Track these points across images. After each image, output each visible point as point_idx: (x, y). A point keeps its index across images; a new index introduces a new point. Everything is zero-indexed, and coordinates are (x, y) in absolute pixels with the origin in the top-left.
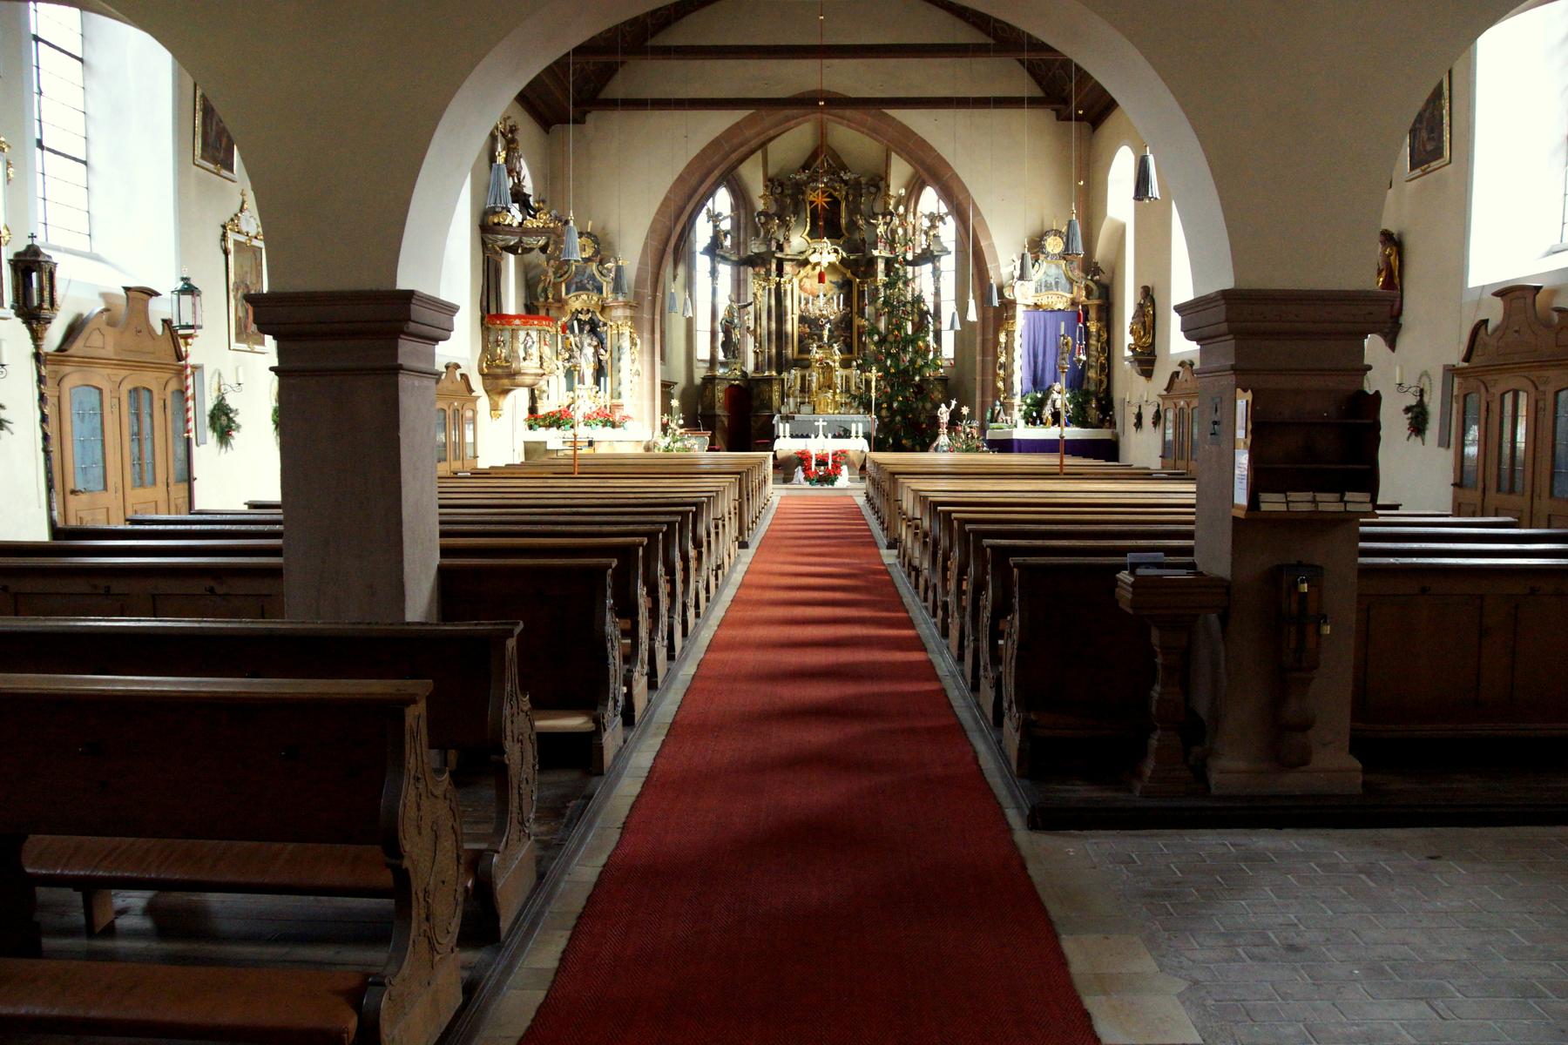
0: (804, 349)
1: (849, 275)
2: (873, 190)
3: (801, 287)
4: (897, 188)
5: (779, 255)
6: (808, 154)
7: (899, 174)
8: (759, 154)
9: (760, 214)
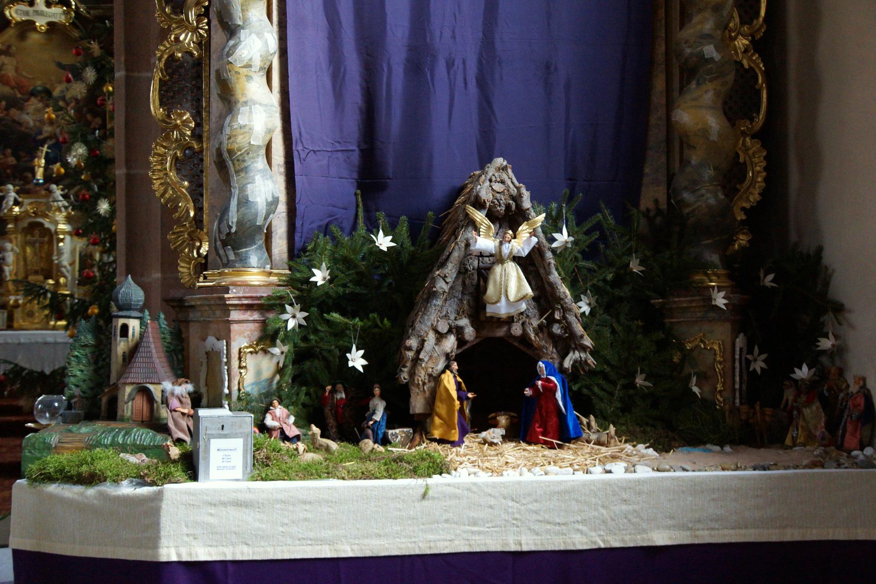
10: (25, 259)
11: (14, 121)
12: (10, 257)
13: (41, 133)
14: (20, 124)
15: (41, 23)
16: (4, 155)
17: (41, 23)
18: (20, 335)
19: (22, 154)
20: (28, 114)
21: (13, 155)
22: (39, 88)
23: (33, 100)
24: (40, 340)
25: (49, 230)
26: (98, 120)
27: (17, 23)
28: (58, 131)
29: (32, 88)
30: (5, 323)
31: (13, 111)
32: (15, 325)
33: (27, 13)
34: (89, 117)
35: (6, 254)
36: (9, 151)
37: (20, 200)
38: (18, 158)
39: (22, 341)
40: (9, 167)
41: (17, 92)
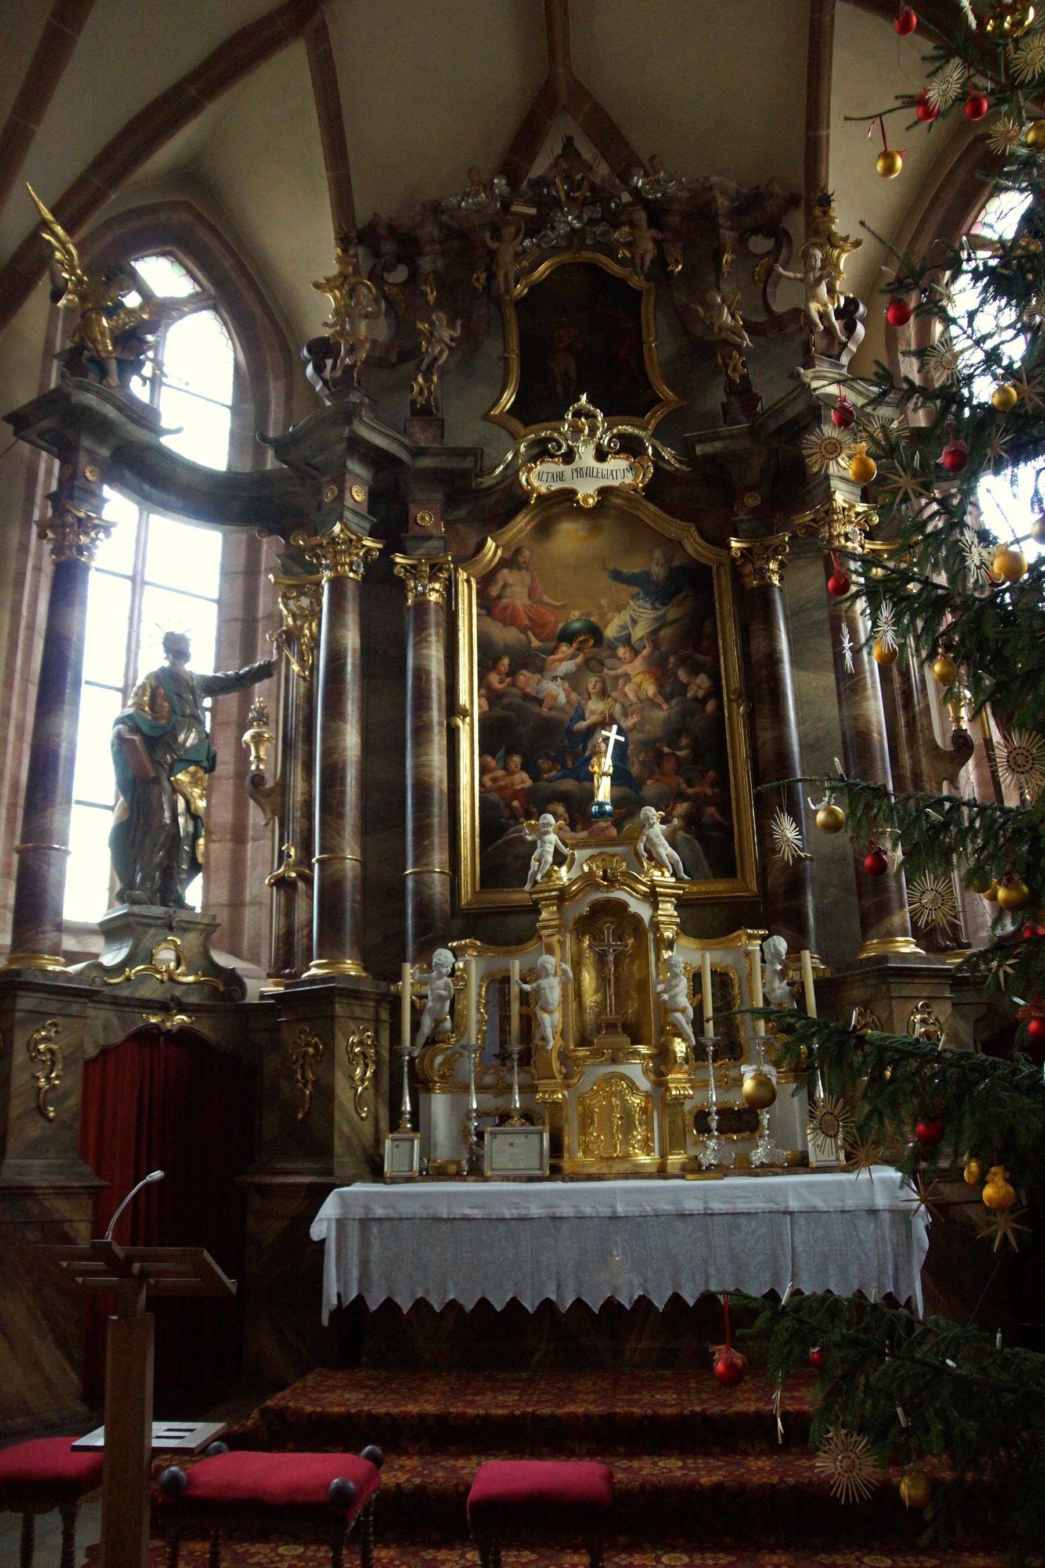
0: (504, 854)
1: (694, 545)
2: (759, 244)
3: (487, 604)
9: (322, 350)
10: (579, 994)
11: (526, 697)
12: (553, 990)
13: (583, 718)
14: (540, 702)
15: (587, 491)
16: (505, 768)
17: (587, 491)
18: (613, 1191)
19: (543, 763)
20: (554, 678)
21: (524, 767)
22: (577, 625)
23: (565, 649)
24: (667, 1207)
25: (637, 918)
26: (703, 681)
27: (539, 496)
28: (618, 708)
29: (561, 626)
30: (547, 1162)
31: (525, 677)
32: (567, 1165)
33: (561, 477)
34: (682, 675)
35: (544, 983)
36: (517, 759)
37: (566, 851)
38: (536, 775)
39: (620, 1210)
40: (516, 794)
41: (532, 638)
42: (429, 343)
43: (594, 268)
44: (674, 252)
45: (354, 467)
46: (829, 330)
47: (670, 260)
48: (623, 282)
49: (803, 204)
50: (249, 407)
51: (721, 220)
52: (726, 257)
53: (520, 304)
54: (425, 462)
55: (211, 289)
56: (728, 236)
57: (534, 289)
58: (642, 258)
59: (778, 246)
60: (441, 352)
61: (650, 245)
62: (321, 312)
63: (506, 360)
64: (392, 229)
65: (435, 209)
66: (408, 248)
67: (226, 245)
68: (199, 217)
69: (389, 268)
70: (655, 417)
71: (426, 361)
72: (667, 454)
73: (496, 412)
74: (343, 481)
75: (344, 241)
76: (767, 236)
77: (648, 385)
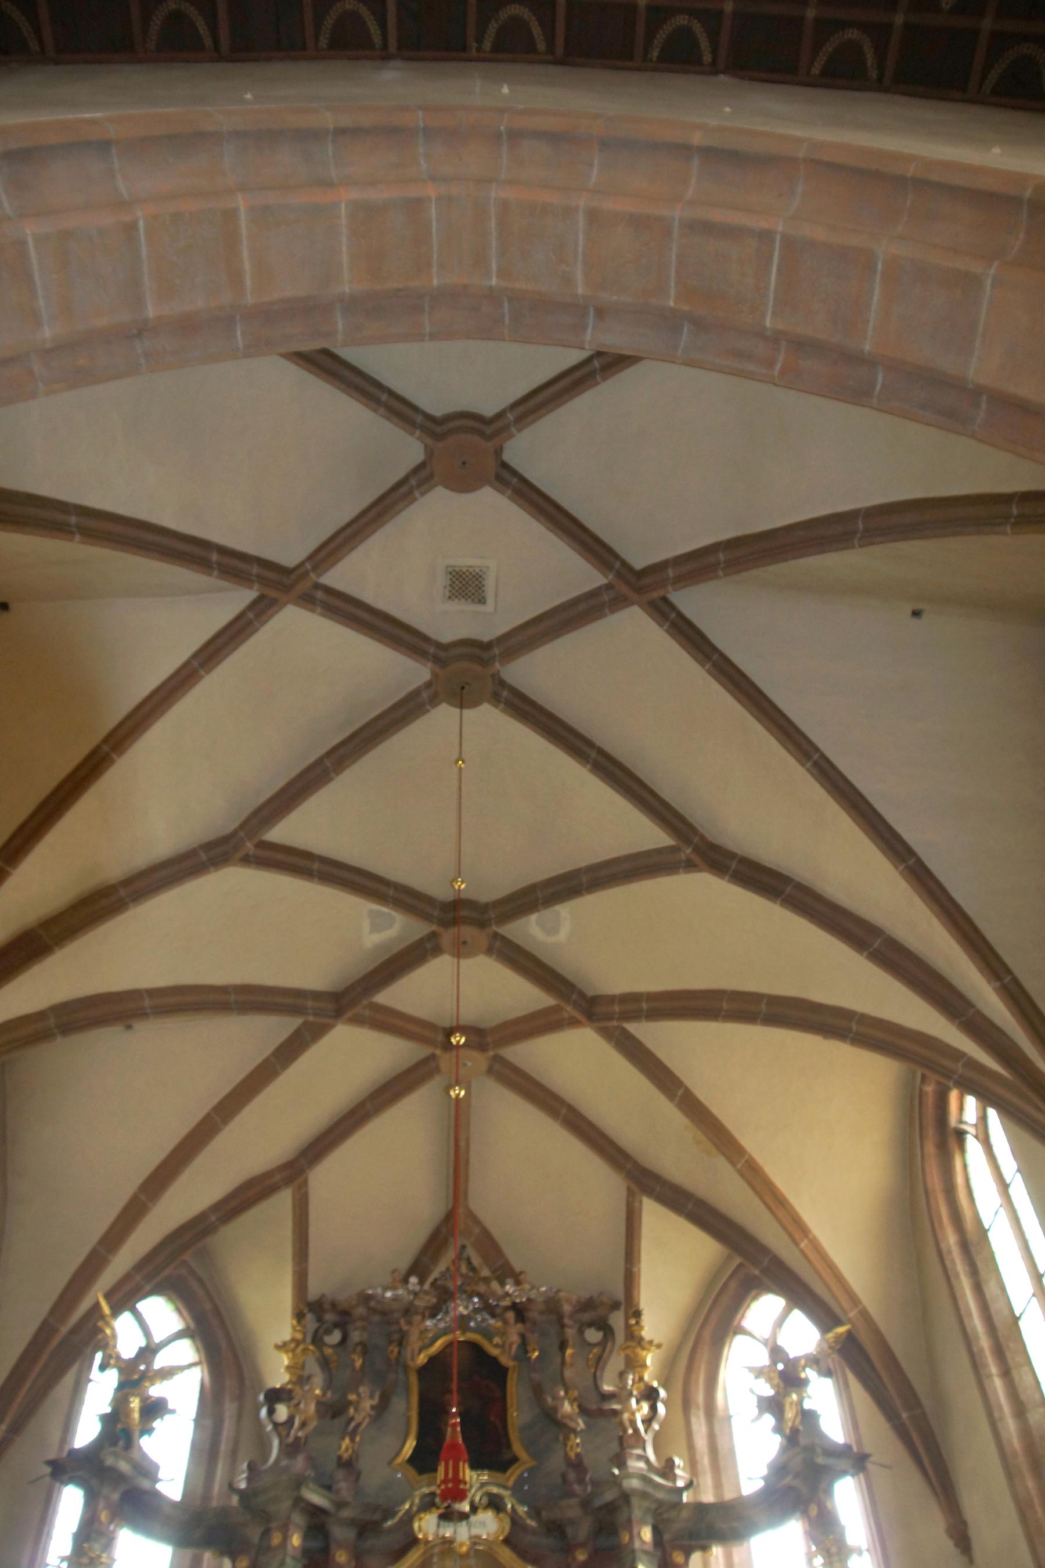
2: (593, 1335)
4: (661, 1309)
5: (316, 1498)
6: (420, 1236)
7: (671, 1268)
8: (285, 1198)
9: (275, 1396)
42: (356, 1410)
43: (474, 1346)
44: (533, 1338)
45: (298, 1519)
46: (636, 1431)
47: (529, 1348)
48: (494, 1360)
49: (623, 1308)
50: (208, 1423)
51: (567, 1321)
52: (569, 1352)
53: (423, 1371)
54: (346, 1513)
55: (192, 1325)
56: (570, 1332)
57: (432, 1360)
58: (510, 1349)
59: (605, 1338)
60: (364, 1419)
61: (514, 1338)
62: (277, 1371)
63: (408, 1419)
64: (334, 1305)
65: (366, 1299)
66: (344, 1318)
67: (207, 1292)
68: (192, 1272)
69: (328, 1332)
70: (513, 1475)
71: (353, 1425)
72: (522, 1510)
73: (399, 1460)
74: (287, 1530)
75: (299, 1316)
76: (599, 1329)
77: (509, 1446)
